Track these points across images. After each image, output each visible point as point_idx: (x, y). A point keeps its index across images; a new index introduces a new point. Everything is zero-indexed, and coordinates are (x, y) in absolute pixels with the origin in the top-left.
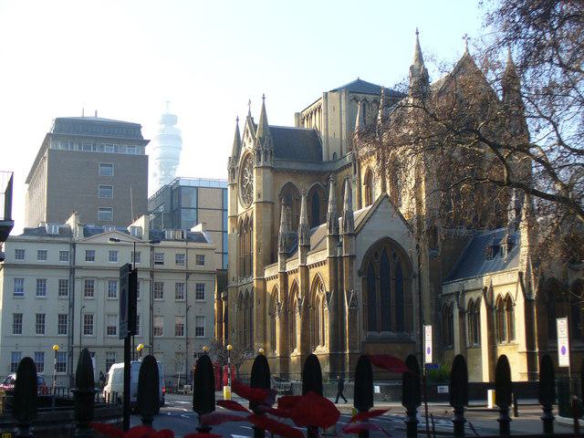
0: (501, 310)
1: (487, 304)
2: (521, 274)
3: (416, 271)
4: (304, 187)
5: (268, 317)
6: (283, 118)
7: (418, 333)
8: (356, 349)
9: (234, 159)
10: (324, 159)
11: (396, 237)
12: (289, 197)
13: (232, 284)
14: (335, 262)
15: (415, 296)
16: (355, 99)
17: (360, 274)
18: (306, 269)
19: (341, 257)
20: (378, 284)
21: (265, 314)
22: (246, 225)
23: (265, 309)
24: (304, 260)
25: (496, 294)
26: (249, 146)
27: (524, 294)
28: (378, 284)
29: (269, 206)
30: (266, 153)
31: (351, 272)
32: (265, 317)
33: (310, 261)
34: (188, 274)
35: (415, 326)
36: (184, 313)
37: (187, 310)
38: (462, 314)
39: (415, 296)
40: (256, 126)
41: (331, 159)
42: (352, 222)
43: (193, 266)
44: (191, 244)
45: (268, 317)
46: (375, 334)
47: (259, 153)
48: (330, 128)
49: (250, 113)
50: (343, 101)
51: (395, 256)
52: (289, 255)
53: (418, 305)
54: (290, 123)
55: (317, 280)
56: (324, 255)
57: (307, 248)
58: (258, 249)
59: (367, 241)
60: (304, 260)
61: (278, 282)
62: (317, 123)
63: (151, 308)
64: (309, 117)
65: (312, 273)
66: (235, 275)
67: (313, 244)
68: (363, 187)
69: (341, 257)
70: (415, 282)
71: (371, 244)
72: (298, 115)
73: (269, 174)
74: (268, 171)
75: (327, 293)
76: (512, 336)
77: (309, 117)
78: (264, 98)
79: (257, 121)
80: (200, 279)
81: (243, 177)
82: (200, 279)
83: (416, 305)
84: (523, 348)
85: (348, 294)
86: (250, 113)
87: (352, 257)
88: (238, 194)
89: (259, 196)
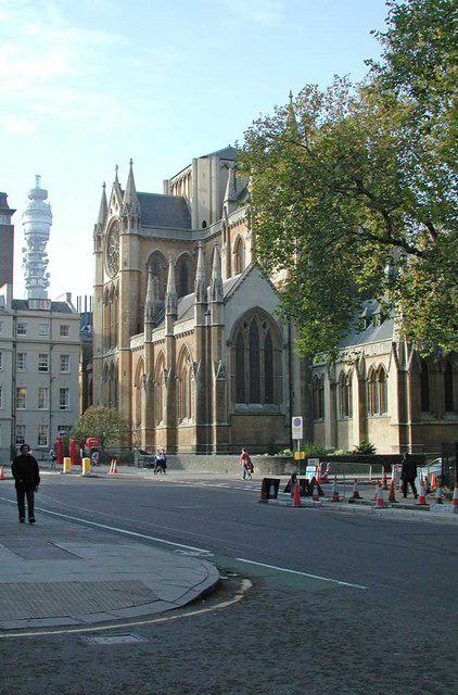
0: (373, 382)
1: (359, 376)
2: (394, 344)
4: (172, 256)
6: (151, 184)
7: (288, 405)
9: (100, 227)
12: (156, 265)
13: (96, 355)
14: (204, 332)
15: (285, 368)
16: (225, 165)
18: (173, 338)
19: (209, 327)
20: (247, 355)
21: (131, 385)
22: (112, 294)
23: (131, 382)
24: (170, 329)
25: (368, 364)
26: (116, 213)
27: (398, 365)
30: (133, 220)
31: (219, 341)
33: (177, 330)
34: (52, 345)
36: (47, 385)
37: (51, 381)
38: (333, 386)
40: (123, 192)
41: (201, 227)
42: (220, 292)
43: (57, 337)
44: (56, 314)
45: (134, 389)
46: (243, 406)
47: (125, 219)
48: (202, 196)
49: (117, 178)
50: (213, 167)
51: (264, 326)
52: (155, 325)
54: (159, 190)
55: (184, 350)
56: (191, 325)
57: (174, 317)
58: (124, 319)
59: (237, 310)
60: (170, 329)
61: (144, 353)
62: (185, 191)
63: (14, 380)
64: (178, 184)
65: (179, 342)
67: (180, 313)
68: (233, 256)
69: (209, 327)
72: (166, 182)
73: (136, 243)
74: (136, 238)
75: (195, 364)
76: (384, 409)
77: (178, 184)
78: (131, 163)
79: (124, 188)
80: (63, 350)
81: (109, 245)
82: (63, 350)
84: (395, 420)
85: (217, 365)
86: (117, 178)
87: (220, 327)
88: (103, 262)
89: (125, 264)
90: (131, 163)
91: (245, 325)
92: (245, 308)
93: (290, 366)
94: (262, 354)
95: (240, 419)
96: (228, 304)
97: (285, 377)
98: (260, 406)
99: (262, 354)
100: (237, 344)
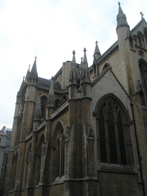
3: (132, 119)
5: (25, 163)
7: (138, 166)
8: (94, 176)
10: (62, 88)
11: (117, 95)
15: (133, 138)
17: (94, 115)
23: (24, 159)
28: (106, 125)
29: (33, 104)
32: (23, 164)
35: (135, 159)
39: (133, 138)
41: (66, 88)
46: (107, 165)
51: (117, 108)
53: (136, 144)
66: (13, 146)
70: (132, 127)
71: (102, 95)
74: (34, 87)
78: (36, 58)
83: (134, 145)
88: (19, 108)
90: (36, 58)
91: (104, 105)
92: (104, 93)
93: (136, 136)
94: (116, 127)
95: (105, 175)
96: (95, 86)
97: (134, 145)
98: (118, 166)
99: (116, 127)
100: (99, 114)
